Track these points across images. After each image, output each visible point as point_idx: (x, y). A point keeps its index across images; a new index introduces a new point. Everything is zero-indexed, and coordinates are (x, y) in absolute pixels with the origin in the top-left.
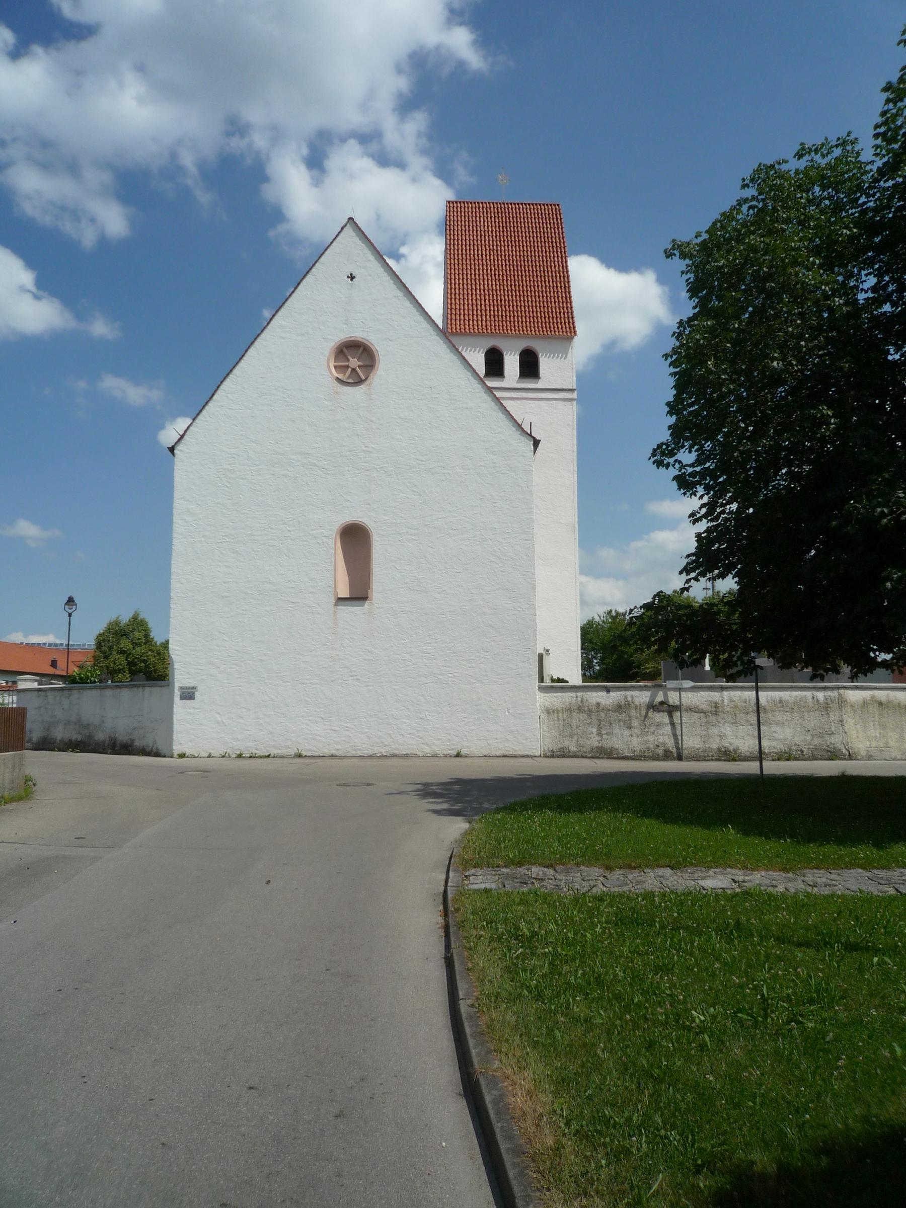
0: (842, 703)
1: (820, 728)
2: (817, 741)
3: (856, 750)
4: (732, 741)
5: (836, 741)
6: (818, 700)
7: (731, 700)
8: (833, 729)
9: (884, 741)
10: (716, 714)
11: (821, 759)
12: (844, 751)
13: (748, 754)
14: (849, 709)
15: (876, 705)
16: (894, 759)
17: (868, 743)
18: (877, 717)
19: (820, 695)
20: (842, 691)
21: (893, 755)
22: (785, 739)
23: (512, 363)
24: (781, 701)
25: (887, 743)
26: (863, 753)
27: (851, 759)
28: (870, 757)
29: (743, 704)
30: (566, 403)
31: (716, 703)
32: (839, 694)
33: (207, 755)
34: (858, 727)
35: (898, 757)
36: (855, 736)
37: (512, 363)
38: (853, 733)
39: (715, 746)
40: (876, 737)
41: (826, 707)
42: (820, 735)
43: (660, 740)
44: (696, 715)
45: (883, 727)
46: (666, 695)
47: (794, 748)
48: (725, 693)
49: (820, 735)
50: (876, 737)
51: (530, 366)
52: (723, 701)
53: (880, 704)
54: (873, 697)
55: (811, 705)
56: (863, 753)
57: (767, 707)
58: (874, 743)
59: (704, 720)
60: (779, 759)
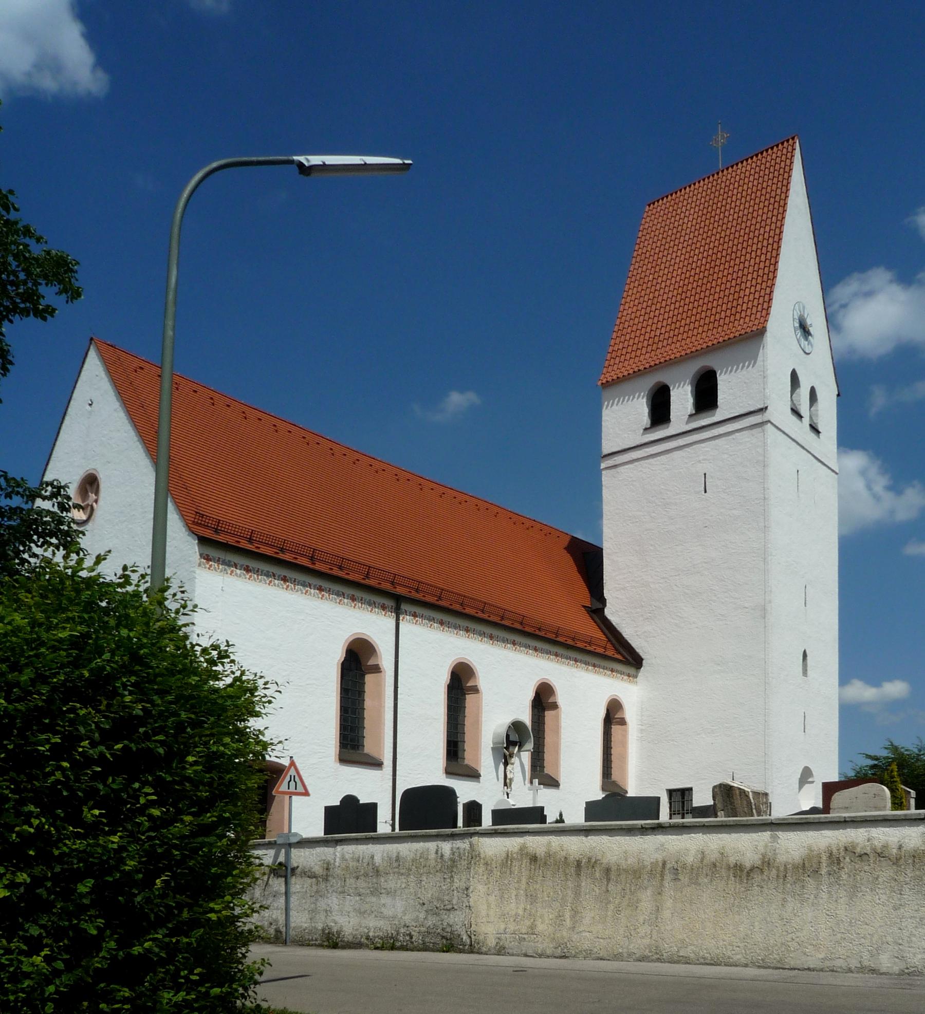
0: (474, 856)
1: (438, 899)
2: (431, 921)
3: (481, 938)
4: (336, 918)
5: (456, 920)
6: (442, 856)
7: (343, 858)
8: (454, 902)
9: (528, 923)
10: (326, 879)
11: (433, 950)
12: (465, 937)
13: (350, 938)
14: (481, 869)
15: (526, 861)
16: (540, 956)
17: (503, 926)
18: (524, 880)
19: (446, 847)
20: (475, 839)
21: (540, 947)
22: (394, 917)
23: (682, 399)
24: (398, 859)
25: (533, 927)
26: (491, 942)
27: (472, 952)
28: (501, 951)
29: (355, 864)
30: (755, 431)
31: (328, 863)
32: (471, 845)
33: (441, 942)
34: (492, 899)
35: (549, 952)
36: (484, 913)
37: (682, 399)
38: (482, 909)
39: (320, 926)
40: (517, 915)
41: (450, 867)
42: (435, 912)
43: (274, 916)
44: (309, 881)
45: (532, 898)
46: (288, 855)
47: (402, 930)
48: (339, 848)
49: (435, 912)
50: (517, 915)
51: (706, 395)
52: (335, 859)
53: (534, 859)
54: (523, 848)
55: (433, 863)
56: (491, 942)
57: (381, 869)
58: (512, 927)
59: (315, 888)
60: (381, 948)
